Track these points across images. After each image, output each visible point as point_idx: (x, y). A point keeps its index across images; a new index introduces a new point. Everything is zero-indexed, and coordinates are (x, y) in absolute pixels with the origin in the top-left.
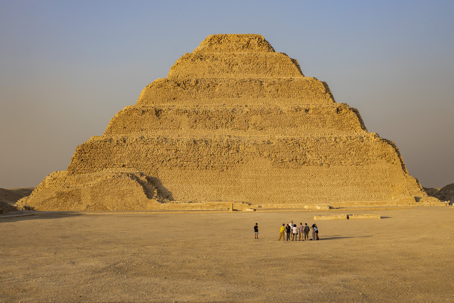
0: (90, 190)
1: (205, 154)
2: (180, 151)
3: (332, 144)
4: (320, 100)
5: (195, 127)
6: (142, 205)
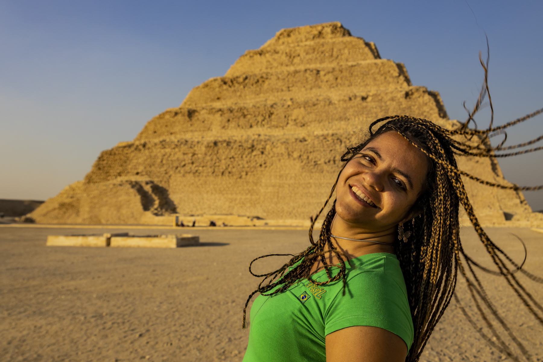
1: (223, 158)
2: (197, 154)
4: (391, 85)
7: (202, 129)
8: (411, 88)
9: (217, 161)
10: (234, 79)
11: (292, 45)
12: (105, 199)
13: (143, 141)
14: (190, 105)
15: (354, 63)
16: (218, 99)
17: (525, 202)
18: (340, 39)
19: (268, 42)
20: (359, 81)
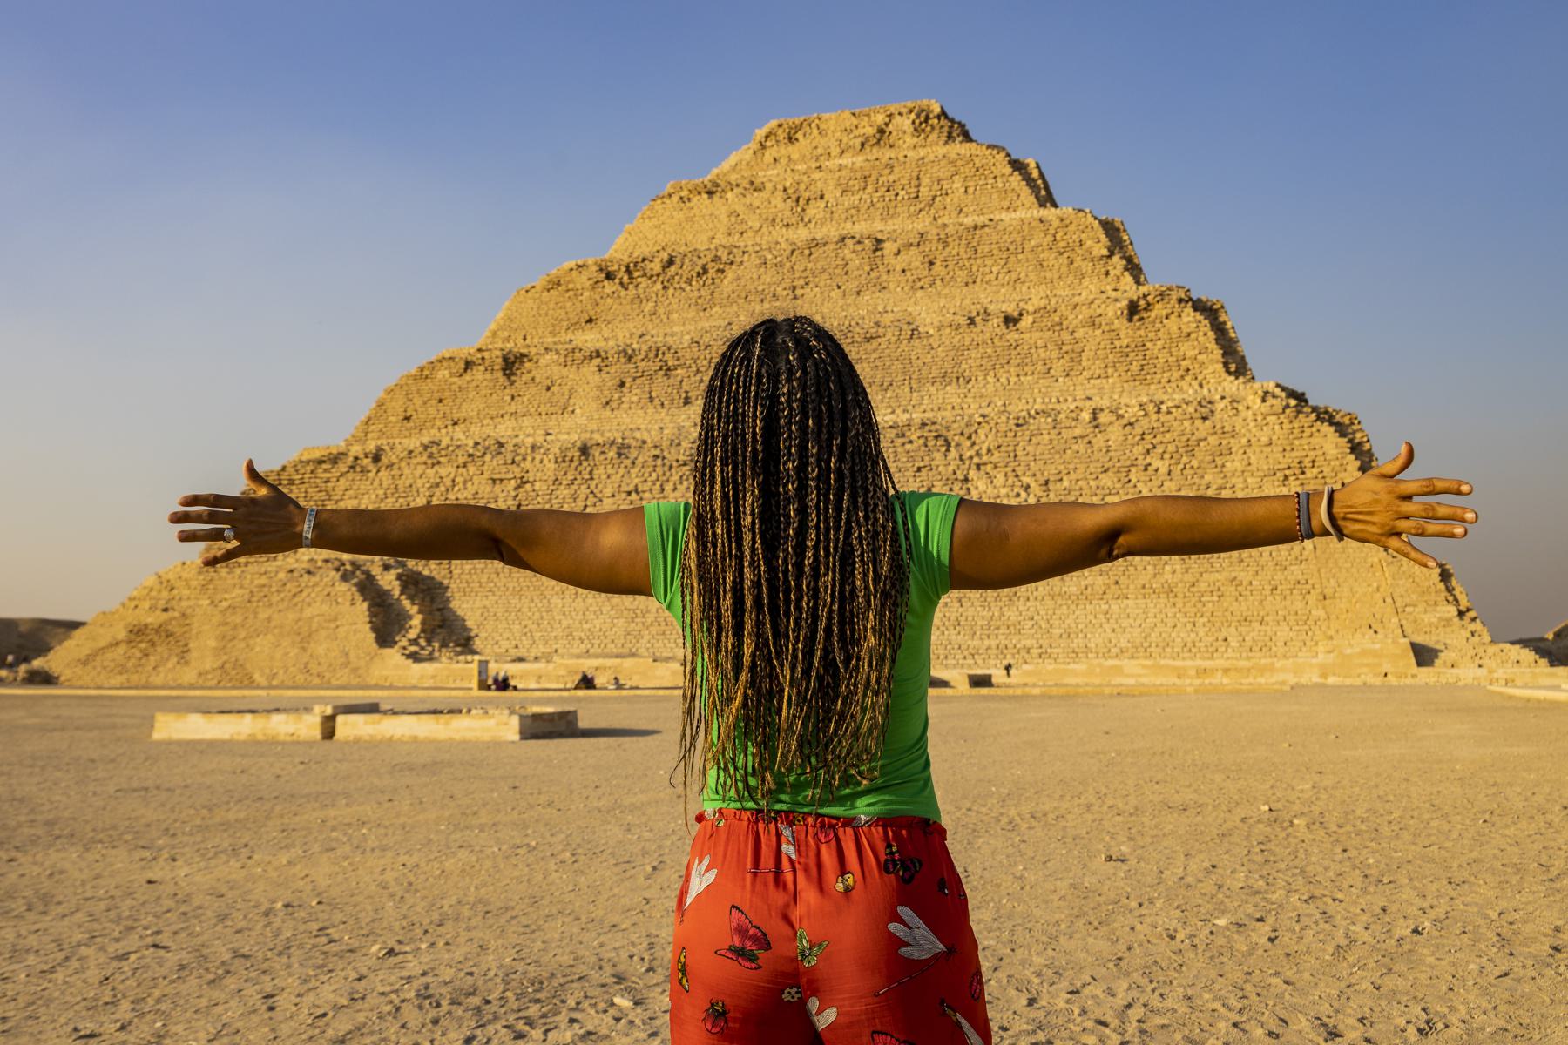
0: (216, 619)
1: (608, 492)
2: (532, 483)
3: (1077, 432)
4: (1086, 282)
5: (614, 405)
6: (355, 670)
7: (542, 409)
8: (1143, 289)
9: (591, 499)
10: (636, 264)
11: (801, 167)
12: (263, 615)
13: (371, 446)
14: (508, 339)
15: (982, 220)
16: (590, 321)
17: (1472, 614)
18: (938, 148)
19: (733, 159)
20: (995, 270)
